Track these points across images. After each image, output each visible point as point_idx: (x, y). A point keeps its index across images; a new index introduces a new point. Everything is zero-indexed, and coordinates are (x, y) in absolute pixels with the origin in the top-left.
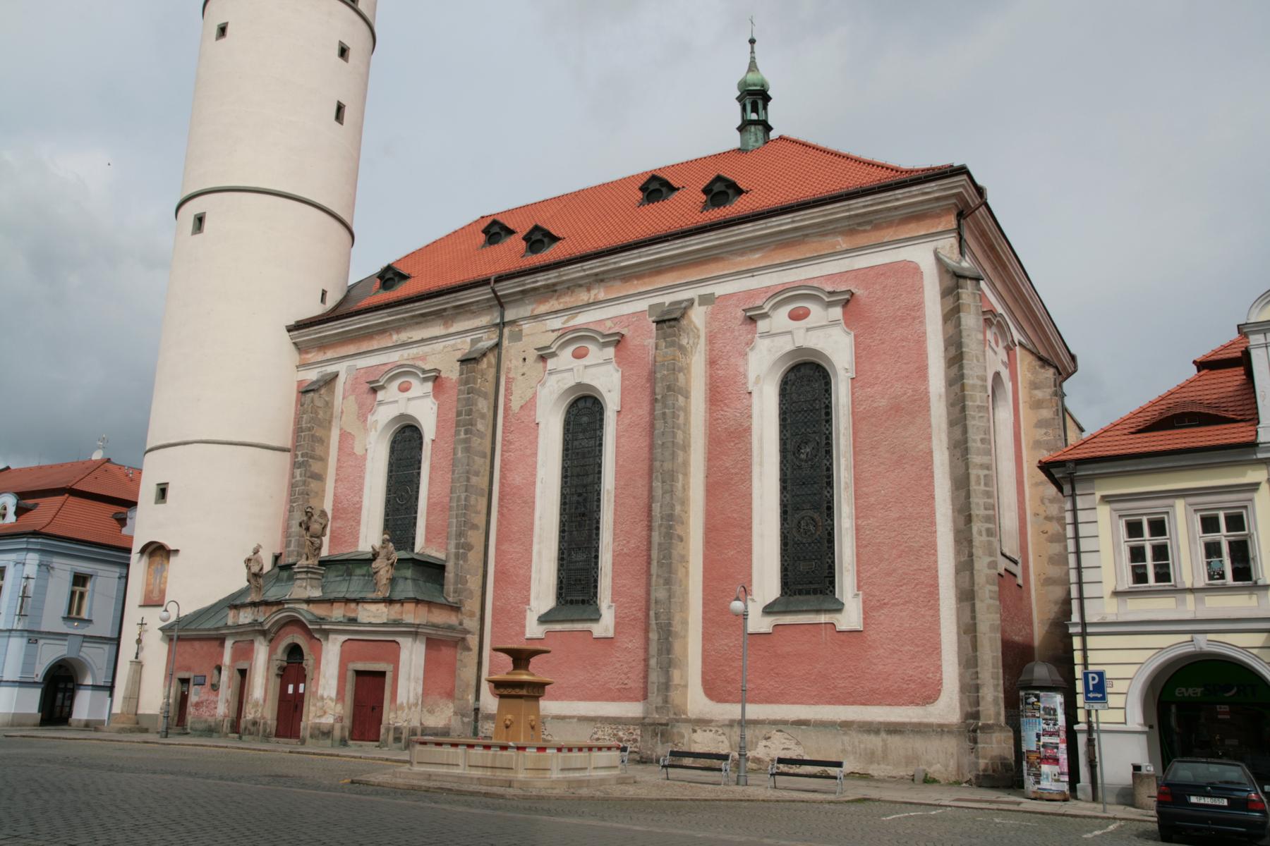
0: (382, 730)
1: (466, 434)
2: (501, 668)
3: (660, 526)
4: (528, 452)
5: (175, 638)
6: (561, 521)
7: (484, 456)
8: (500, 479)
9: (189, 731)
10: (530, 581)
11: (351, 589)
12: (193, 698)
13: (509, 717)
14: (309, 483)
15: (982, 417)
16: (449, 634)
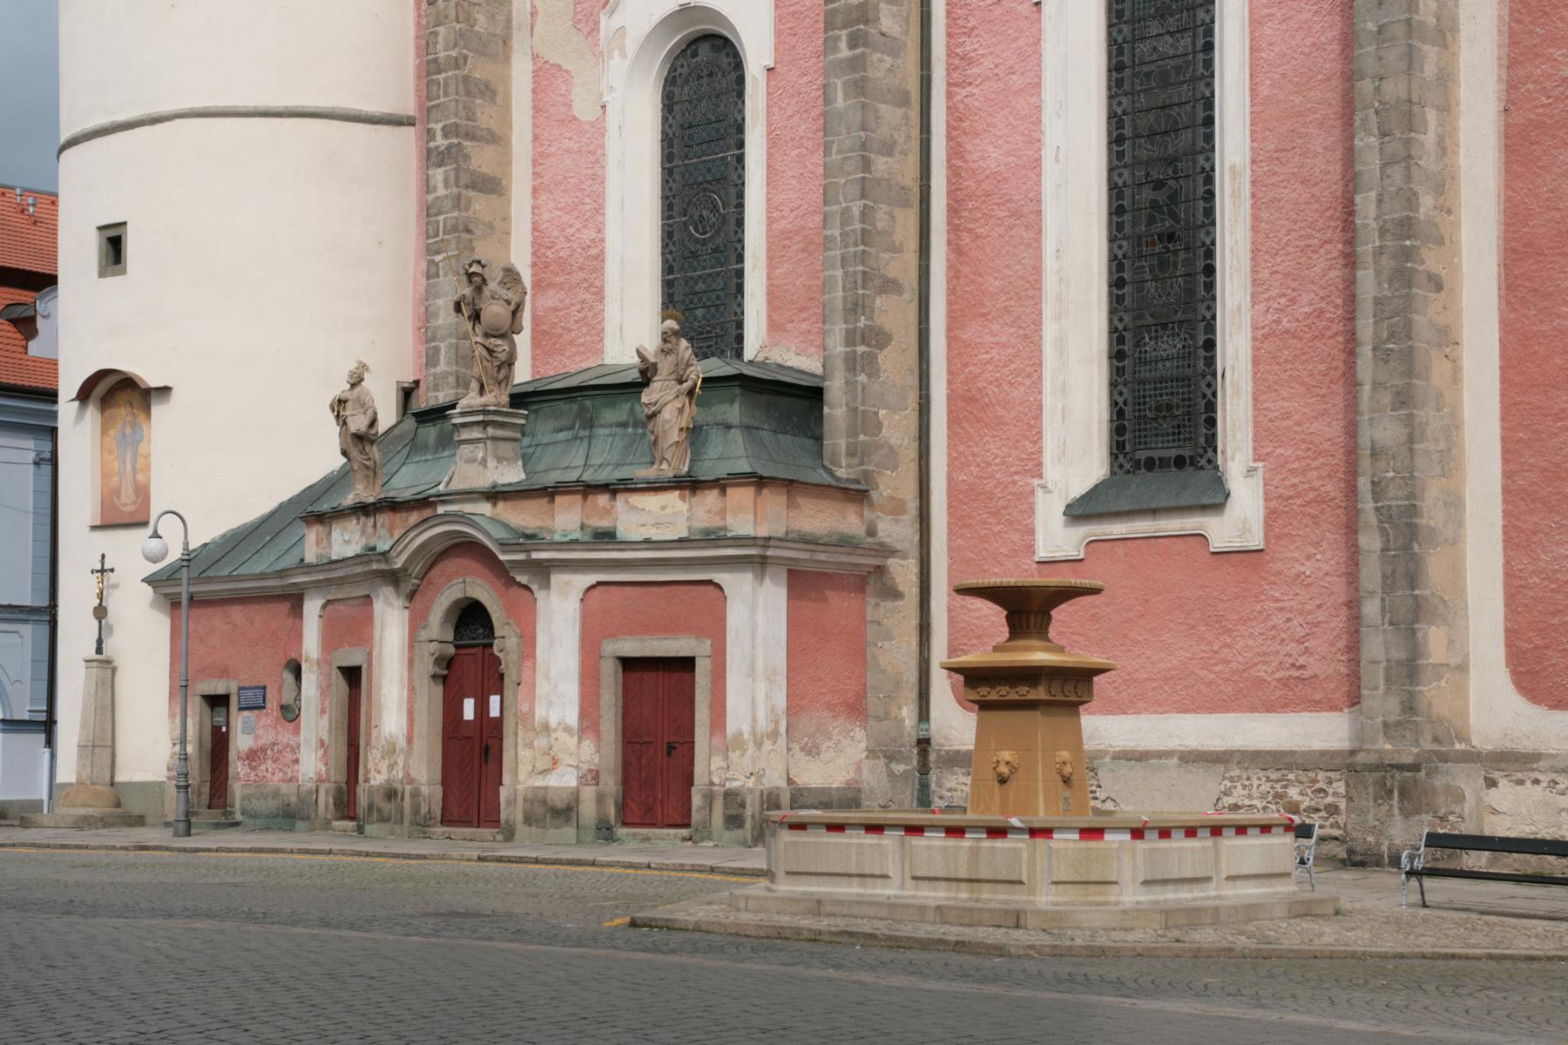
0: (697, 800)
1: (852, 46)
2: (979, 637)
3: (1380, 252)
4: (1017, 81)
5: (185, 601)
6: (1113, 258)
7: (904, 101)
8: (949, 160)
9: (239, 817)
10: (1039, 416)
11: (596, 460)
12: (241, 742)
13: (1006, 755)
14: (469, 201)
16: (844, 559)
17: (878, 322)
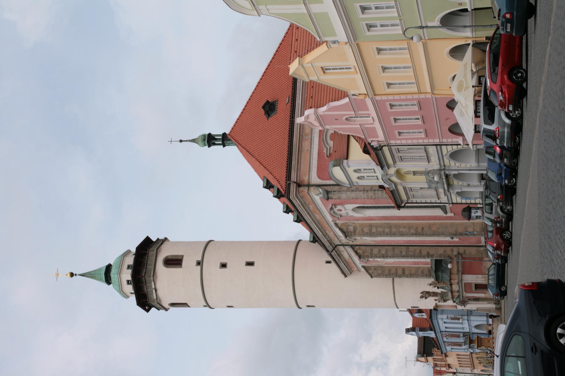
7: (394, 249)
14: (407, 274)
15: (377, 193)
17: (426, 254)
